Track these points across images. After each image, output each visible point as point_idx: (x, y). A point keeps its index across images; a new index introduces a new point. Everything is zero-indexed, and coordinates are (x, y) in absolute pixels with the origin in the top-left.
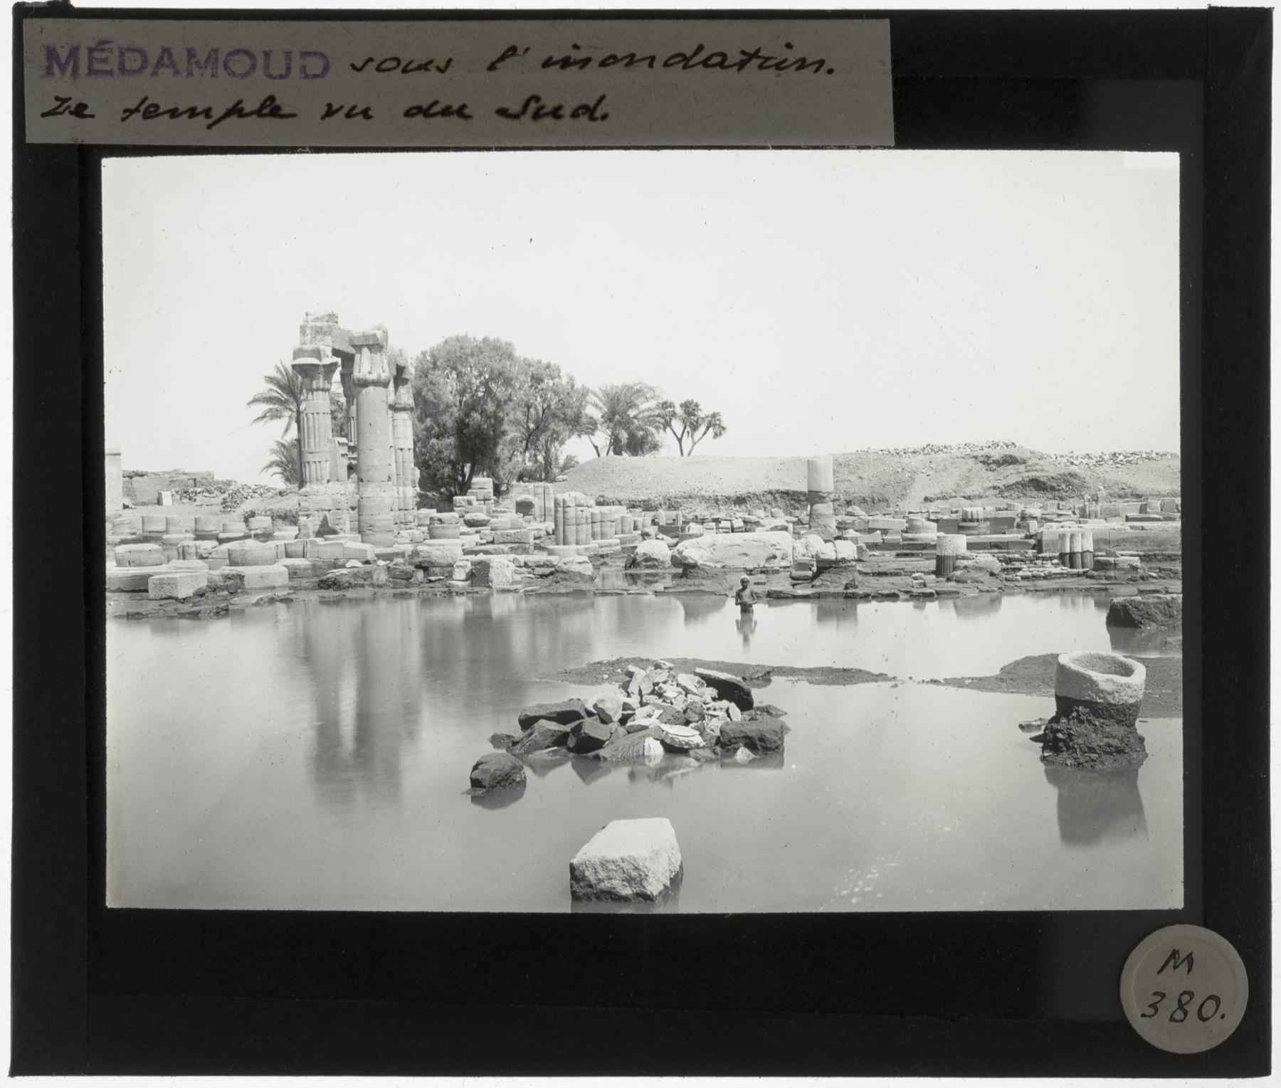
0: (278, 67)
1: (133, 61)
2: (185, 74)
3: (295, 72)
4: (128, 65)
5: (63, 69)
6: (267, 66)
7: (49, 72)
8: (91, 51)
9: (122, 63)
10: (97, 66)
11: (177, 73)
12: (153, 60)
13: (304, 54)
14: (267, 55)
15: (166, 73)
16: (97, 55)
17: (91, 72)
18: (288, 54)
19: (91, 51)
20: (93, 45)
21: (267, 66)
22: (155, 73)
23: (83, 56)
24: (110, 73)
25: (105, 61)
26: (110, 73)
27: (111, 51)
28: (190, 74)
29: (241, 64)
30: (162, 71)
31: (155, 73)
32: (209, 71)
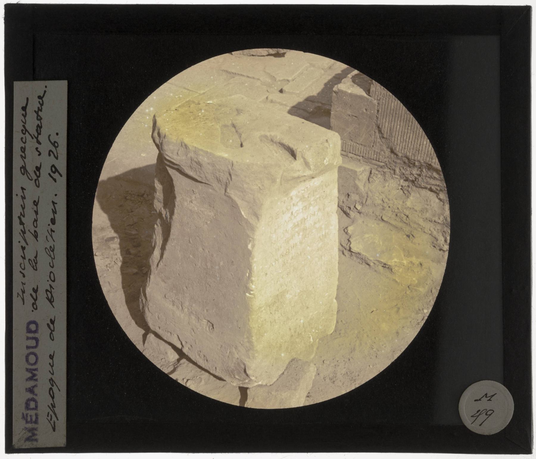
0: (33, 343)
1: (32, 405)
2: (36, 382)
3: (36, 335)
4: (34, 407)
5: (34, 435)
6: (33, 347)
7: (36, 440)
8: (27, 422)
9: (33, 409)
10: (34, 418)
11: (36, 386)
12: (30, 396)
13: (29, 331)
14: (28, 347)
15: (36, 390)
16: (29, 419)
17: (36, 422)
18: (28, 338)
19: (27, 422)
20: (25, 421)
21: (33, 347)
22: (36, 395)
23: (29, 426)
24: (36, 415)
25: (31, 416)
26: (36, 415)
27: (27, 415)
28: (36, 380)
29: (32, 359)
30: (35, 393)
31: (36, 395)
32: (35, 372)
